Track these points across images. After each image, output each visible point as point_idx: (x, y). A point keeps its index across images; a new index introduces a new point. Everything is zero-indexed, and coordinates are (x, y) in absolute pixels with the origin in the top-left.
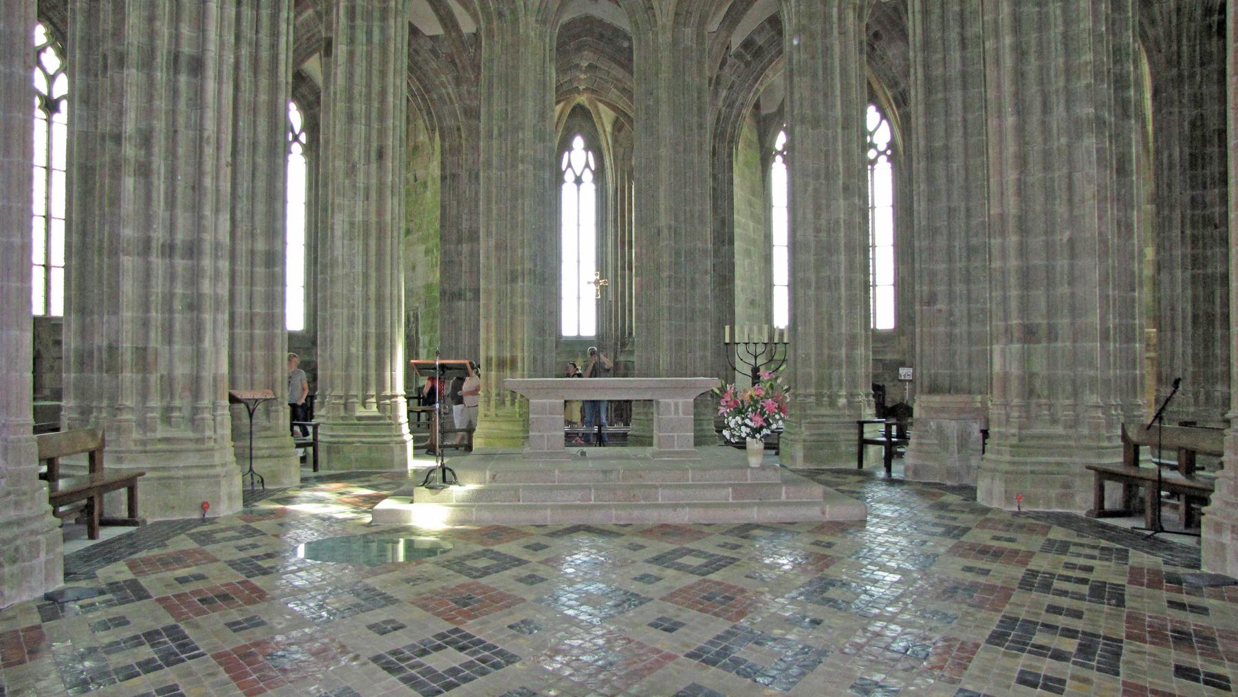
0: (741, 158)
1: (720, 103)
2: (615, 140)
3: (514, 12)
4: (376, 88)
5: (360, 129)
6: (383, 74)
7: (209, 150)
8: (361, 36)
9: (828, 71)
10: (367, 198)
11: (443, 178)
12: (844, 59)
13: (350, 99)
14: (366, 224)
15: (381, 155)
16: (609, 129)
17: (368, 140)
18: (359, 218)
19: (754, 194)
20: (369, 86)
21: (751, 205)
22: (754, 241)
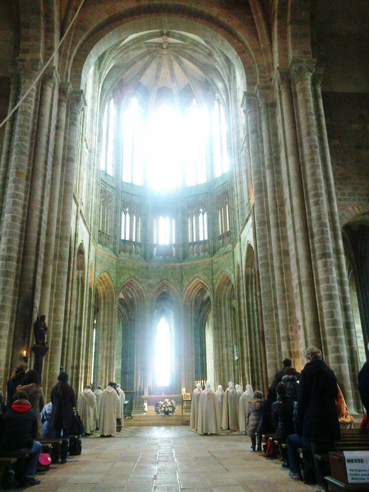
3: (144, 299)
4: (110, 322)
5: (106, 332)
6: (112, 318)
7: (82, 346)
8: (107, 309)
9: (221, 316)
10: (107, 350)
11: (123, 338)
12: (225, 313)
13: (103, 325)
14: (107, 357)
15: (111, 339)
17: (108, 335)
18: (105, 355)
20: (108, 321)
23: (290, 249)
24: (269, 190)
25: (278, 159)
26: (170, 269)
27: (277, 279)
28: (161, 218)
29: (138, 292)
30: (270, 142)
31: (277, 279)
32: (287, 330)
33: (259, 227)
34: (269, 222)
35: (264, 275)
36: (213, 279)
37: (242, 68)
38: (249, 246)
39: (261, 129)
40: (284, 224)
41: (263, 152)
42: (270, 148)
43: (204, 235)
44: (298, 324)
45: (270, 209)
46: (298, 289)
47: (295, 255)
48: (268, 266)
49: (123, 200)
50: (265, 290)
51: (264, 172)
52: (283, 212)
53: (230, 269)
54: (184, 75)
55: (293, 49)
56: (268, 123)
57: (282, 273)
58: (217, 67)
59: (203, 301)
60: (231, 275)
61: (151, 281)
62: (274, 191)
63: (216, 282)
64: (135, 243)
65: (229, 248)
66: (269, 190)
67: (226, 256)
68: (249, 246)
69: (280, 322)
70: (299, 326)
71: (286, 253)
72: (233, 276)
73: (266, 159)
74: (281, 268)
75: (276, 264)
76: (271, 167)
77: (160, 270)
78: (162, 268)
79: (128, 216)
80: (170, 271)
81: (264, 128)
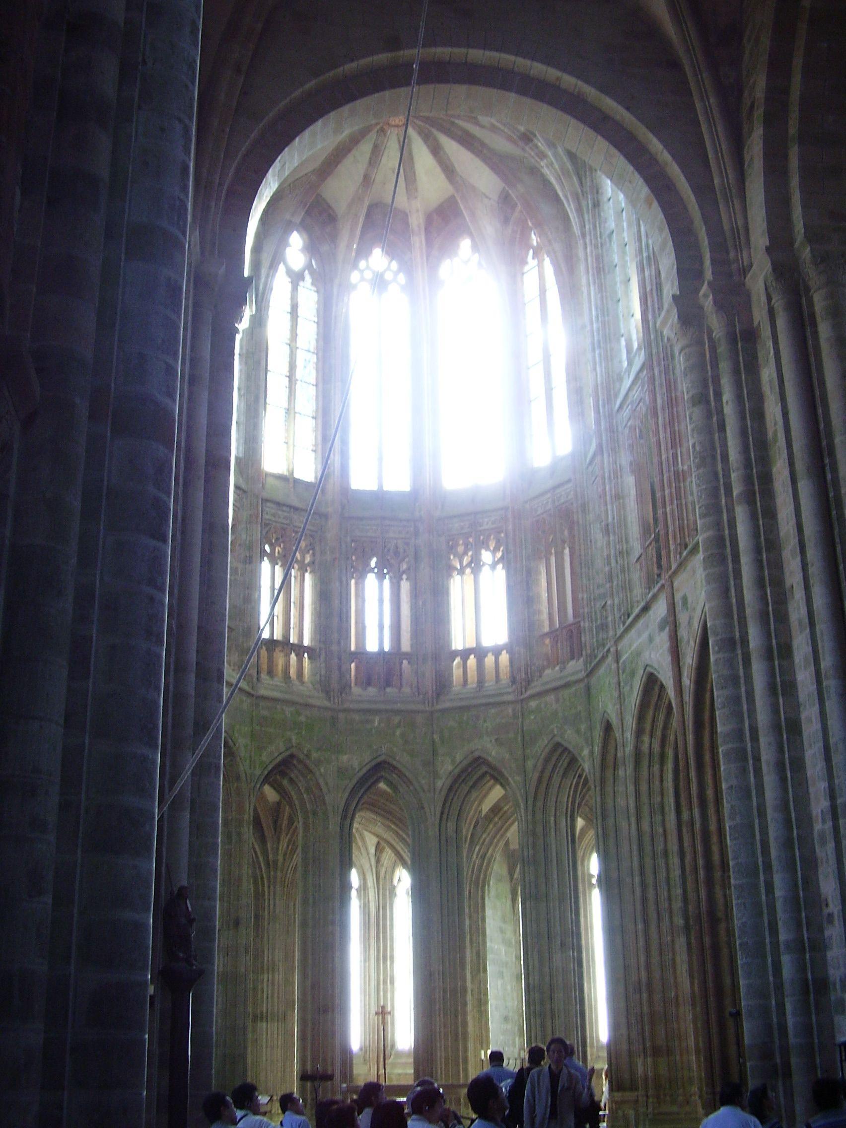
0: (493, 893)
1: (475, 856)
2: (378, 861)
15: (237, 923)
16: (372, 850)
19: (505, 922)
21: (502, 931)
22: (507, 963)
23: (803, 716)
24: (746, 561)
25: (766, 479)
26: (399, 725)
27: (771, 794)
28: (371, 580)
29: (308, 790)
30: (743, 433)
31: (771, 794)
32: (799, 925)
33: (720, 655)
34: (745, 641)
35: (734, 782)
36: (525, 758)
37: (661, 230)
38: (652, 682)
39: (718, 395)
40: (786, 651)
41: (725, 457)
42: (745, 450)
43: (496, 630)
44: (826, 911)
45: (748, 611)
46: (829, 824)
47: (820, 734)
48: (745, 759)
49: (266, 525)
50: (738, 820)
51: (731, 510)
52: (782, 618)
53: (578, 732)
54: (443, 176)
55: (804, 207)
56: (738, 384)
57: (783, 780)
58: (546, 171)
59: (481, 812)
60: (582, 749)
61: (345, 758)
62: (758, 563)
63: (535, 766)
64: (299, 649)
65: (577, 672)
66: (746, 561)
67: (566, 693)
68: (652, 682)
69: (779, 905)
70: (830, 916)
71: (795, 727)
72: (586, 752)
73: (735, 476)
74: (780, 766)
75: (767, 755)
76: (749, 497)
77: (369, 727)
78: (376, 723)
79: (278, 569)
80: (398, 732)
81: (727, 396)
